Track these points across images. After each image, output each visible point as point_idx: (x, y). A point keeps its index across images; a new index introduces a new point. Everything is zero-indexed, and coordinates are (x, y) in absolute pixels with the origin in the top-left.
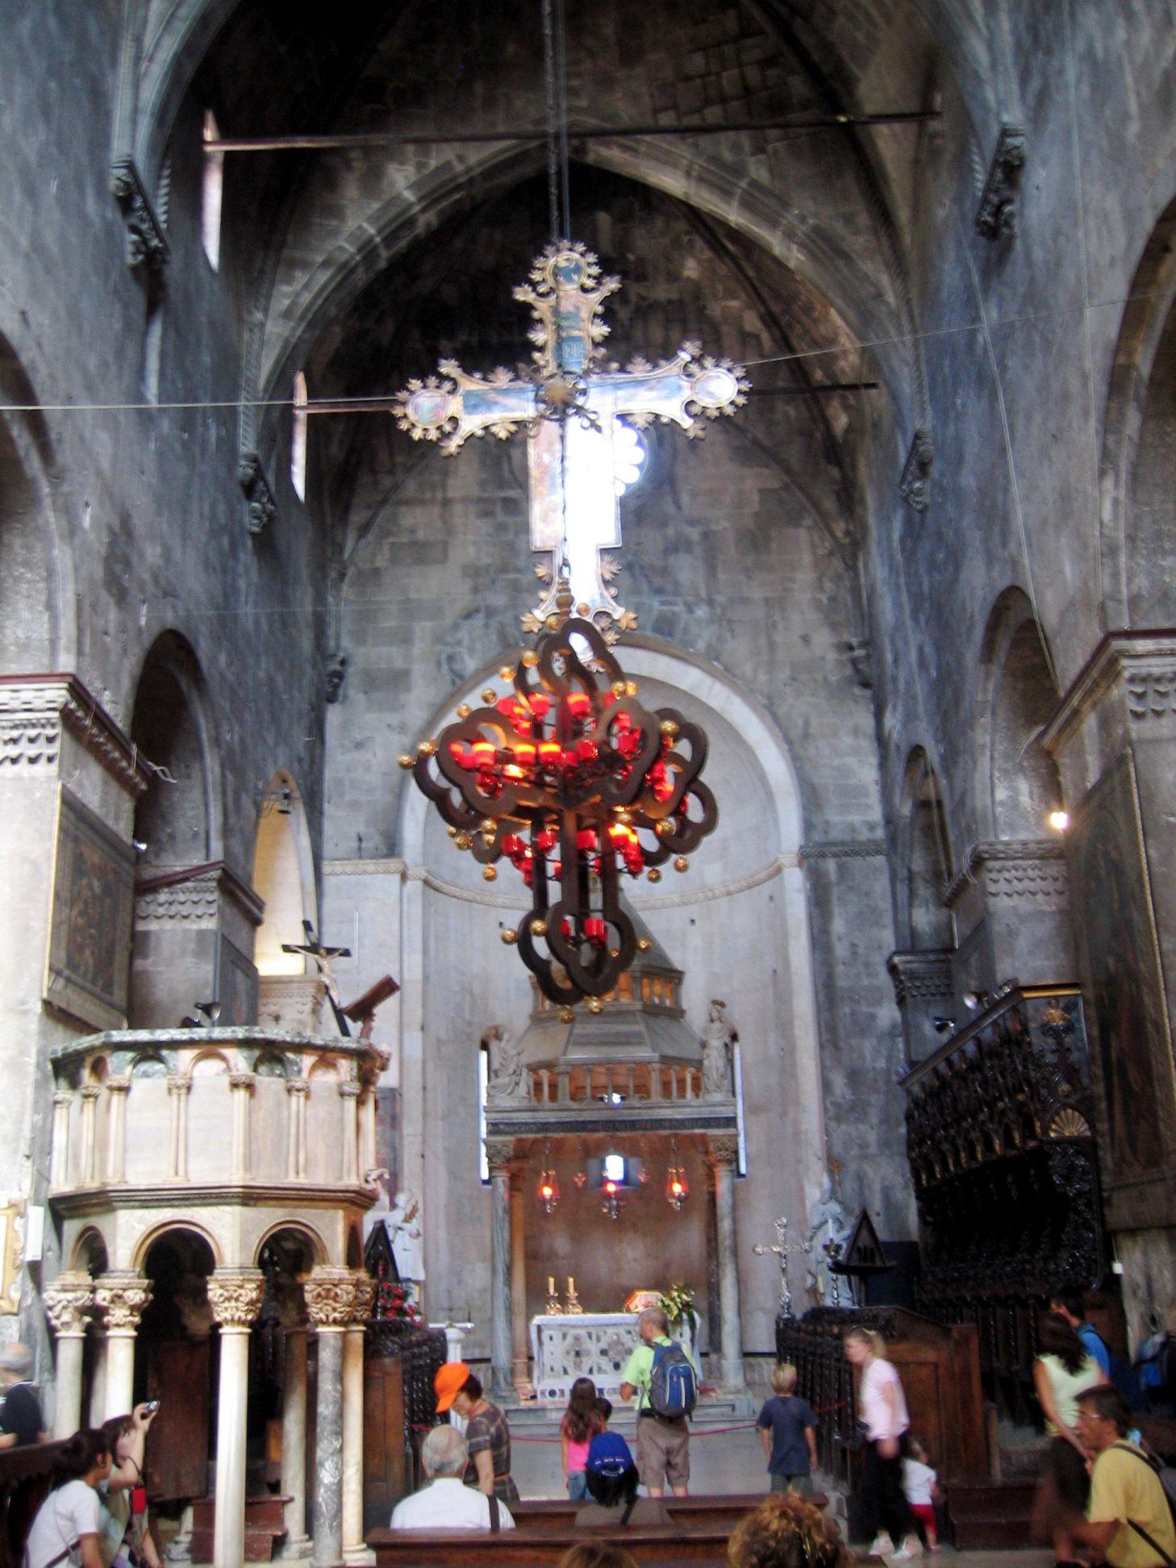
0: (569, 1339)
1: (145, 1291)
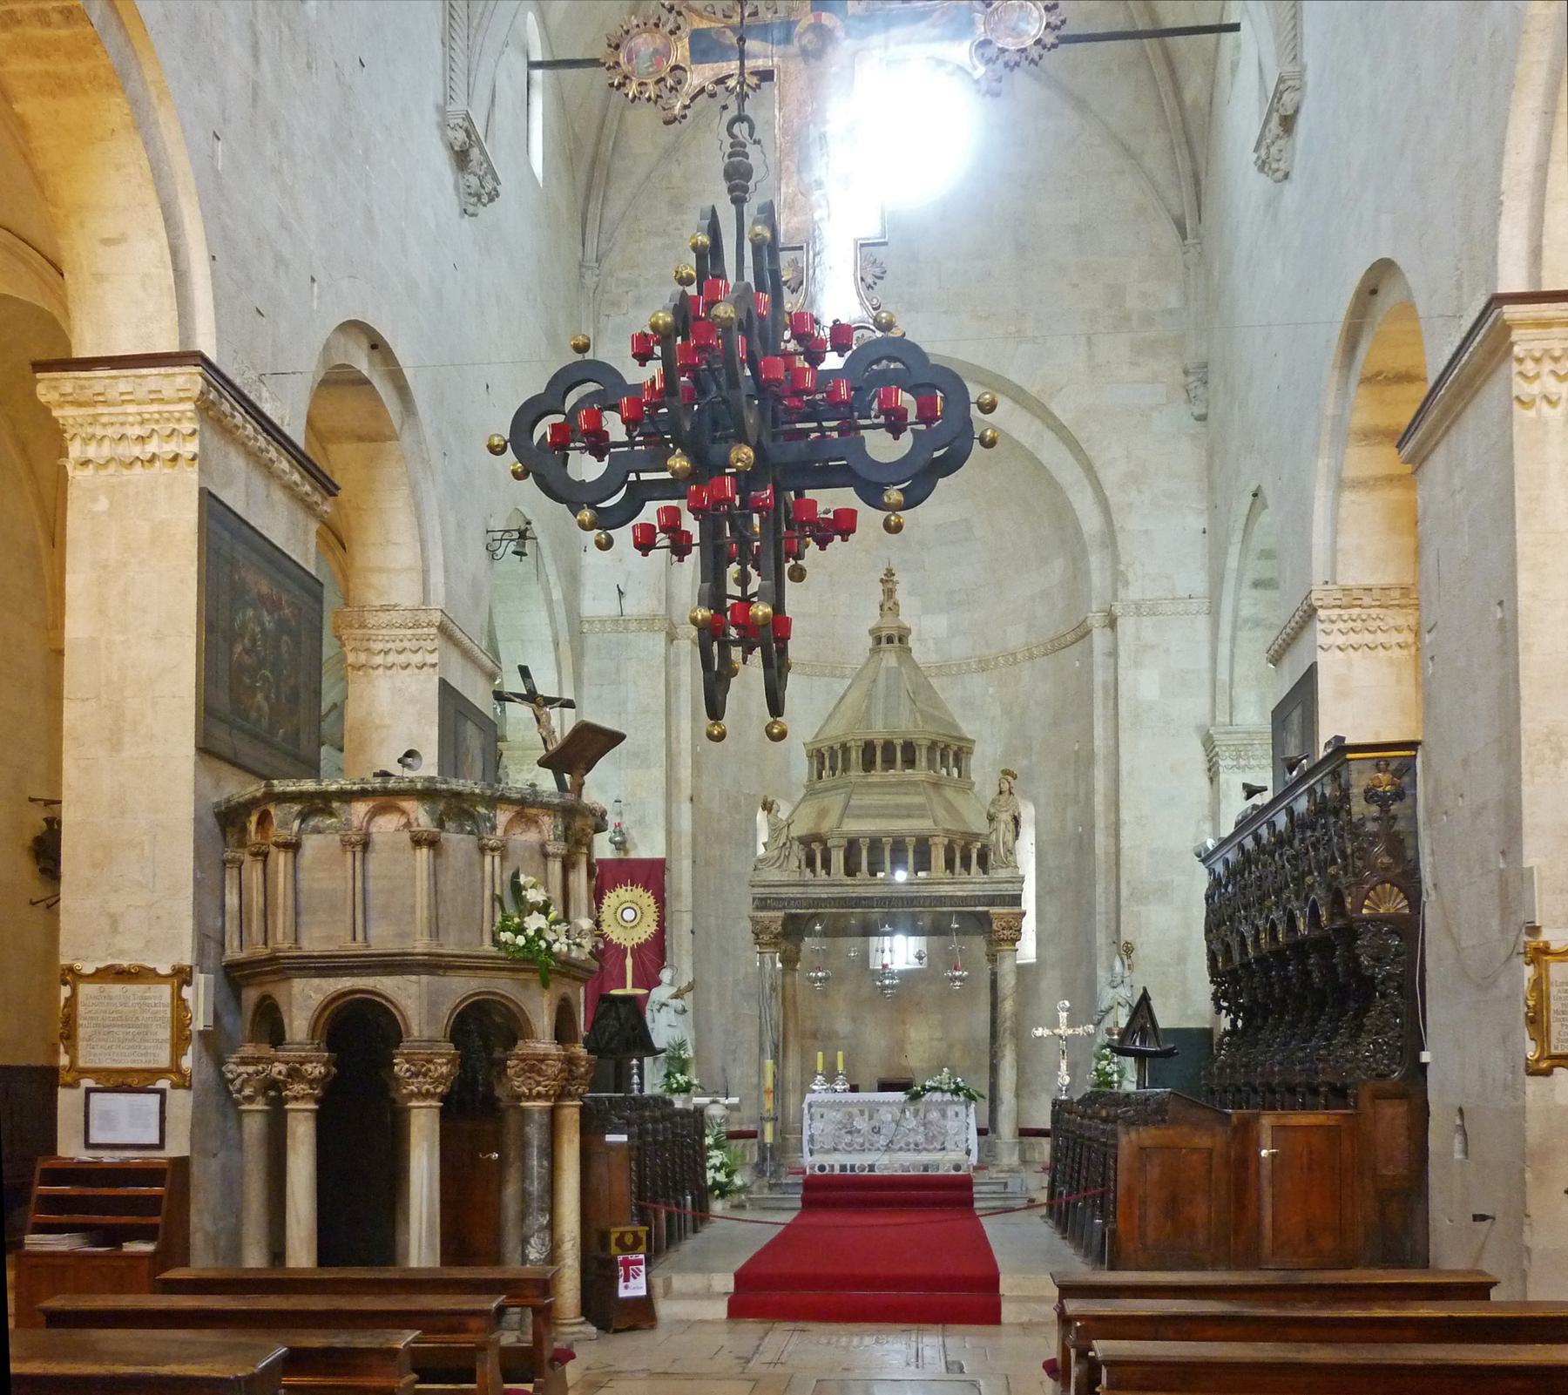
1: (324, 1065)
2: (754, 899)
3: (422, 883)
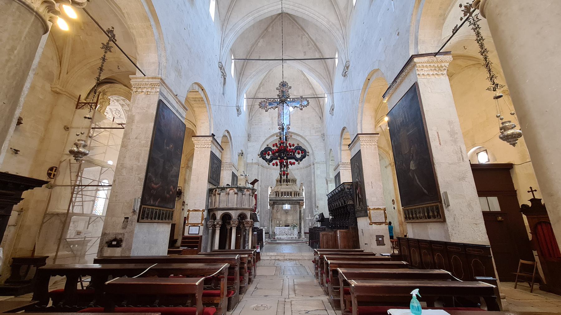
3: (236, 199)
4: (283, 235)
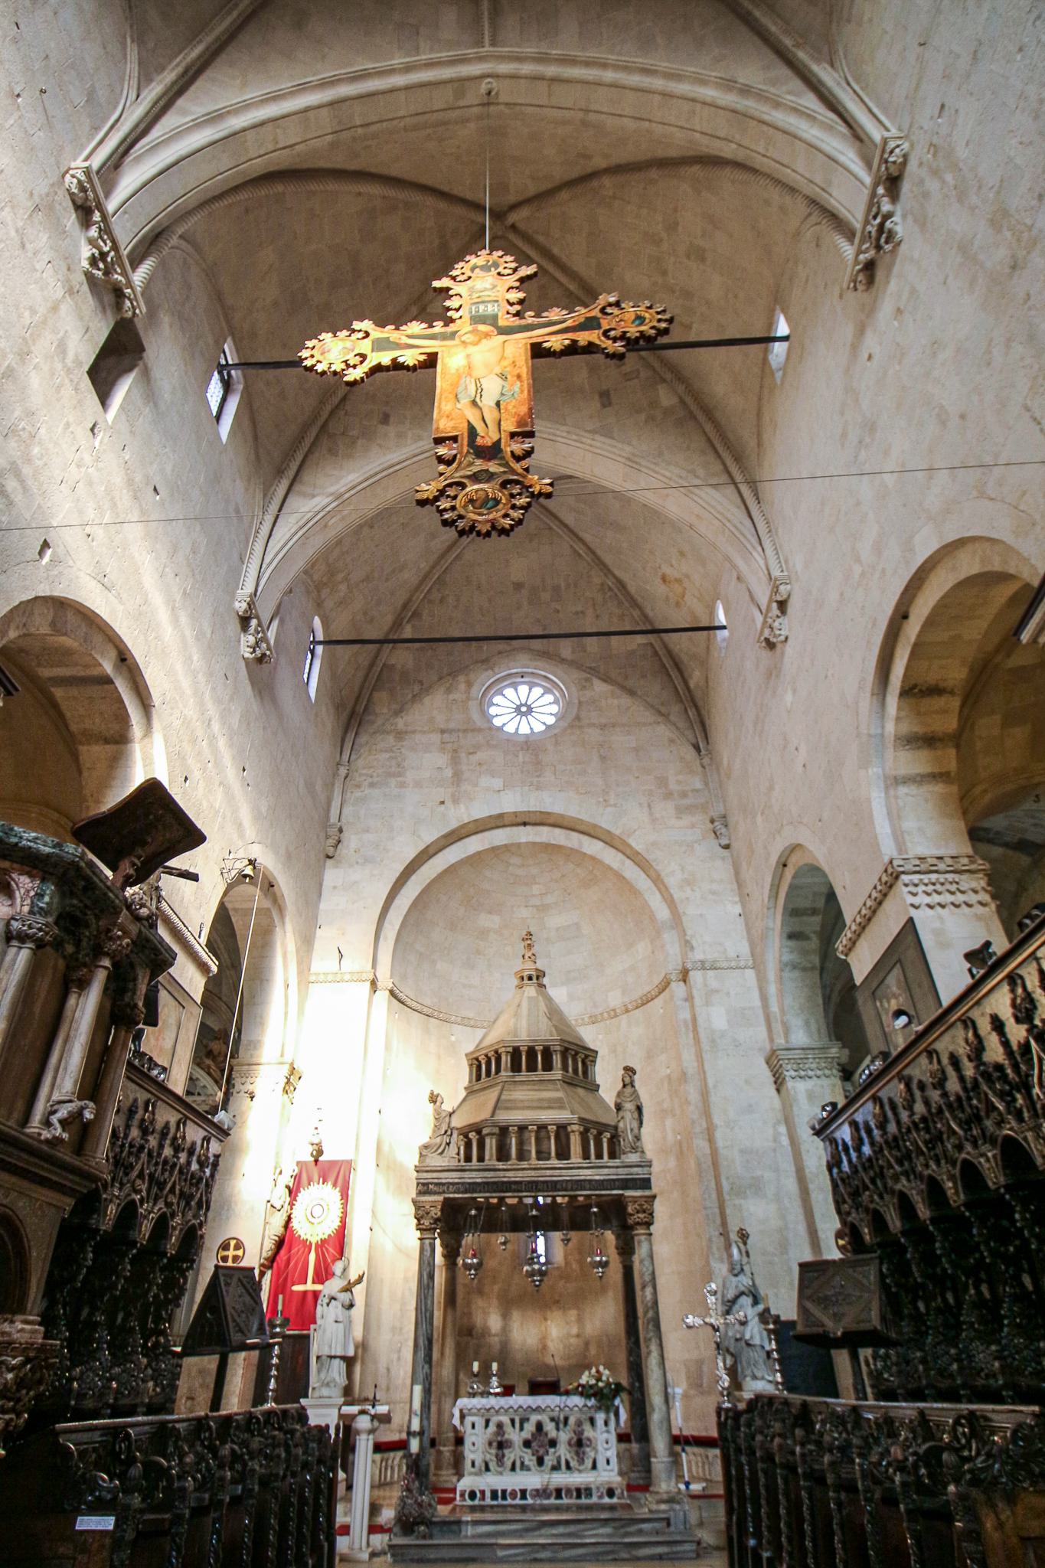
0: (492, 1428)
2: (418, 1184)
4: (513, 1469)
